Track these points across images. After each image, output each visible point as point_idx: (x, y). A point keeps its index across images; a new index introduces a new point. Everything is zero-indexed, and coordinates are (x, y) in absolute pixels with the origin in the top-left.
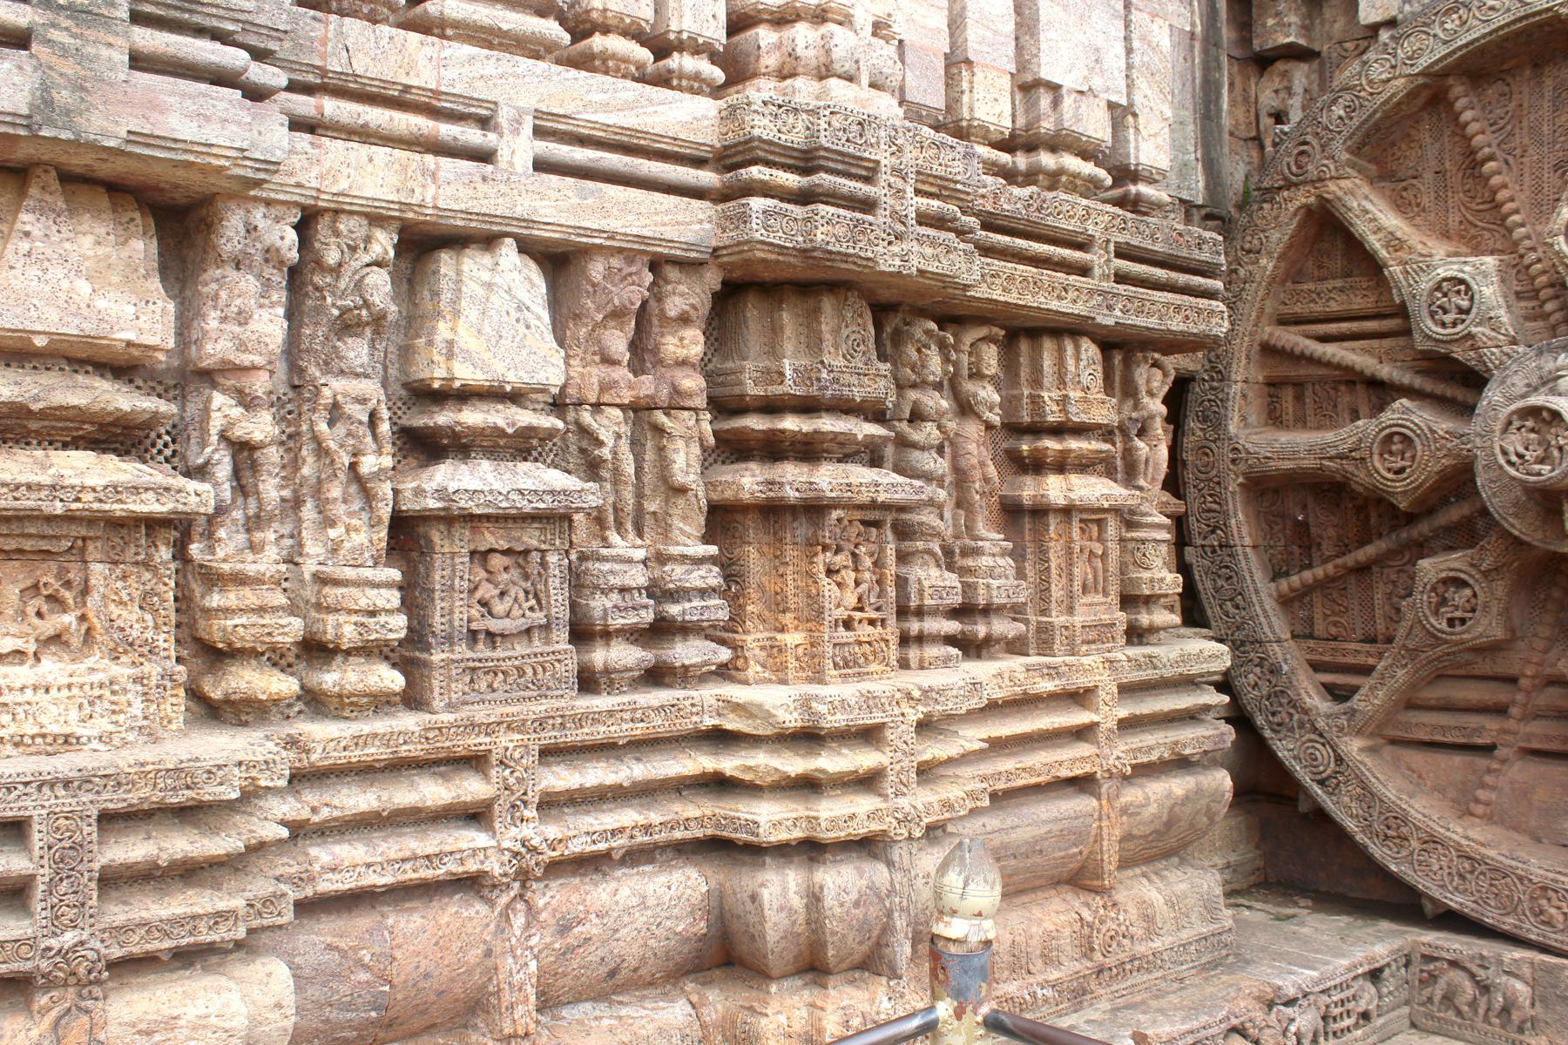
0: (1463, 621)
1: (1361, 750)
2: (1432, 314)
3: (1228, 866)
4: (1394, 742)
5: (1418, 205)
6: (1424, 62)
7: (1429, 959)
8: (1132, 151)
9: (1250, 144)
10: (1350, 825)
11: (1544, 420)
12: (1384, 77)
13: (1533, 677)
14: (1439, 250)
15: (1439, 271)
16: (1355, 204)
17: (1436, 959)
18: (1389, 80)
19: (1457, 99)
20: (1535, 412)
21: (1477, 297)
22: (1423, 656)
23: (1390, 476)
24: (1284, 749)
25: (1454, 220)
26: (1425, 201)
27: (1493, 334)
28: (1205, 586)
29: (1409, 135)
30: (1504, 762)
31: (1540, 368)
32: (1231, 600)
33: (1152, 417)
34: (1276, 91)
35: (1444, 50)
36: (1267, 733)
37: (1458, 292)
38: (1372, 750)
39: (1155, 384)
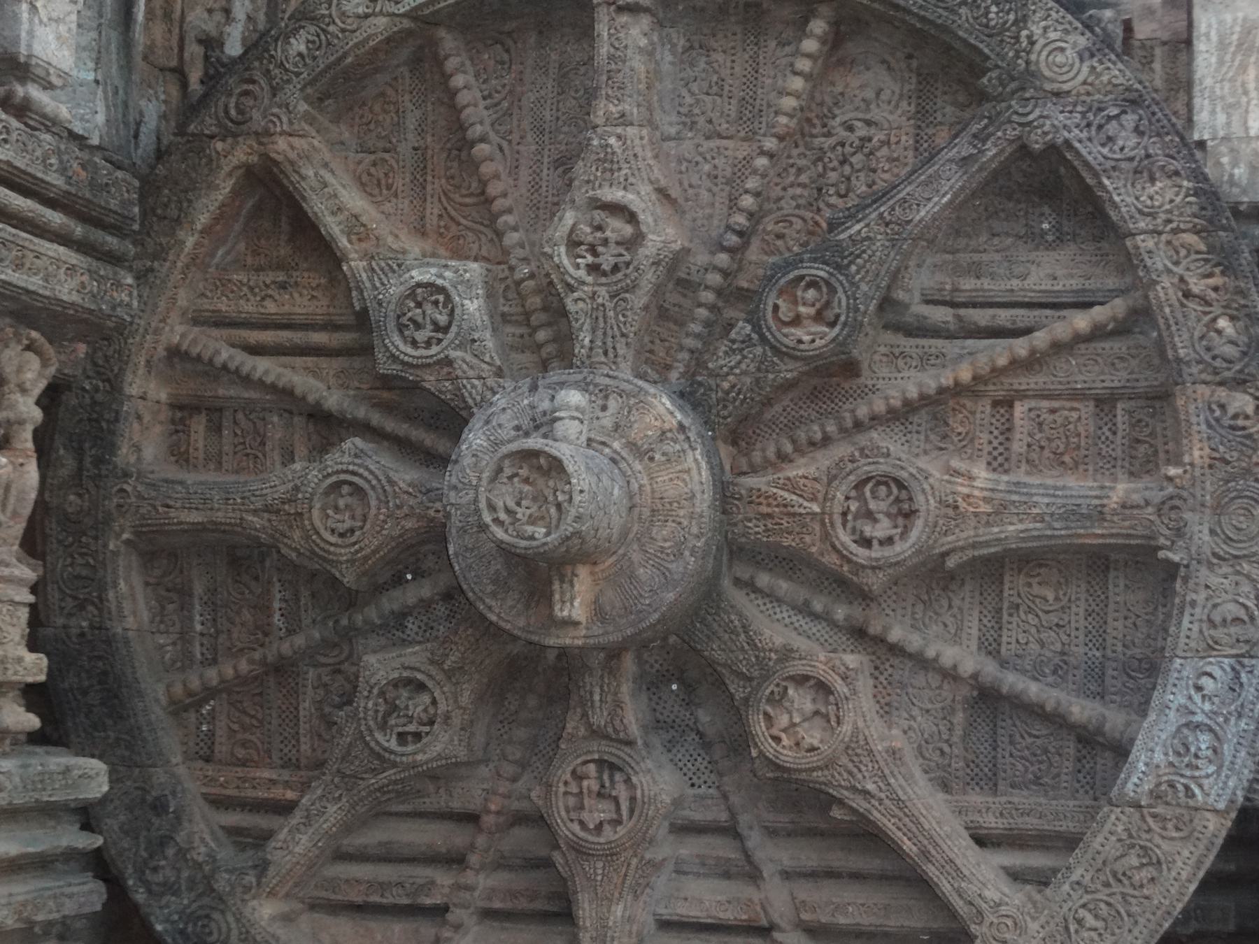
0: (417, 736)
1: (273, 918)
2: (401, 328)
4: (313, 907)
5: (389, 187)
8: (23, 34)
9: (169, 75)
11: (540, 468)
12: (360, 10)
13: (498, 813)
14: (415, 247)
15: (414, 273)
16: (311, 173)
18: (367, 16)
20: (529, 455)
21: (458, 311)
23: (333, 539)
25: (433, 210)
26: (398, 183)
27: (475, 361)
29: (383, 94)
30: (457, 927)
31: (533, 407)
33: (21, 422)
34: (210, 11)
37: (436, 303)
38: (287, 918)
39: (29, 375)
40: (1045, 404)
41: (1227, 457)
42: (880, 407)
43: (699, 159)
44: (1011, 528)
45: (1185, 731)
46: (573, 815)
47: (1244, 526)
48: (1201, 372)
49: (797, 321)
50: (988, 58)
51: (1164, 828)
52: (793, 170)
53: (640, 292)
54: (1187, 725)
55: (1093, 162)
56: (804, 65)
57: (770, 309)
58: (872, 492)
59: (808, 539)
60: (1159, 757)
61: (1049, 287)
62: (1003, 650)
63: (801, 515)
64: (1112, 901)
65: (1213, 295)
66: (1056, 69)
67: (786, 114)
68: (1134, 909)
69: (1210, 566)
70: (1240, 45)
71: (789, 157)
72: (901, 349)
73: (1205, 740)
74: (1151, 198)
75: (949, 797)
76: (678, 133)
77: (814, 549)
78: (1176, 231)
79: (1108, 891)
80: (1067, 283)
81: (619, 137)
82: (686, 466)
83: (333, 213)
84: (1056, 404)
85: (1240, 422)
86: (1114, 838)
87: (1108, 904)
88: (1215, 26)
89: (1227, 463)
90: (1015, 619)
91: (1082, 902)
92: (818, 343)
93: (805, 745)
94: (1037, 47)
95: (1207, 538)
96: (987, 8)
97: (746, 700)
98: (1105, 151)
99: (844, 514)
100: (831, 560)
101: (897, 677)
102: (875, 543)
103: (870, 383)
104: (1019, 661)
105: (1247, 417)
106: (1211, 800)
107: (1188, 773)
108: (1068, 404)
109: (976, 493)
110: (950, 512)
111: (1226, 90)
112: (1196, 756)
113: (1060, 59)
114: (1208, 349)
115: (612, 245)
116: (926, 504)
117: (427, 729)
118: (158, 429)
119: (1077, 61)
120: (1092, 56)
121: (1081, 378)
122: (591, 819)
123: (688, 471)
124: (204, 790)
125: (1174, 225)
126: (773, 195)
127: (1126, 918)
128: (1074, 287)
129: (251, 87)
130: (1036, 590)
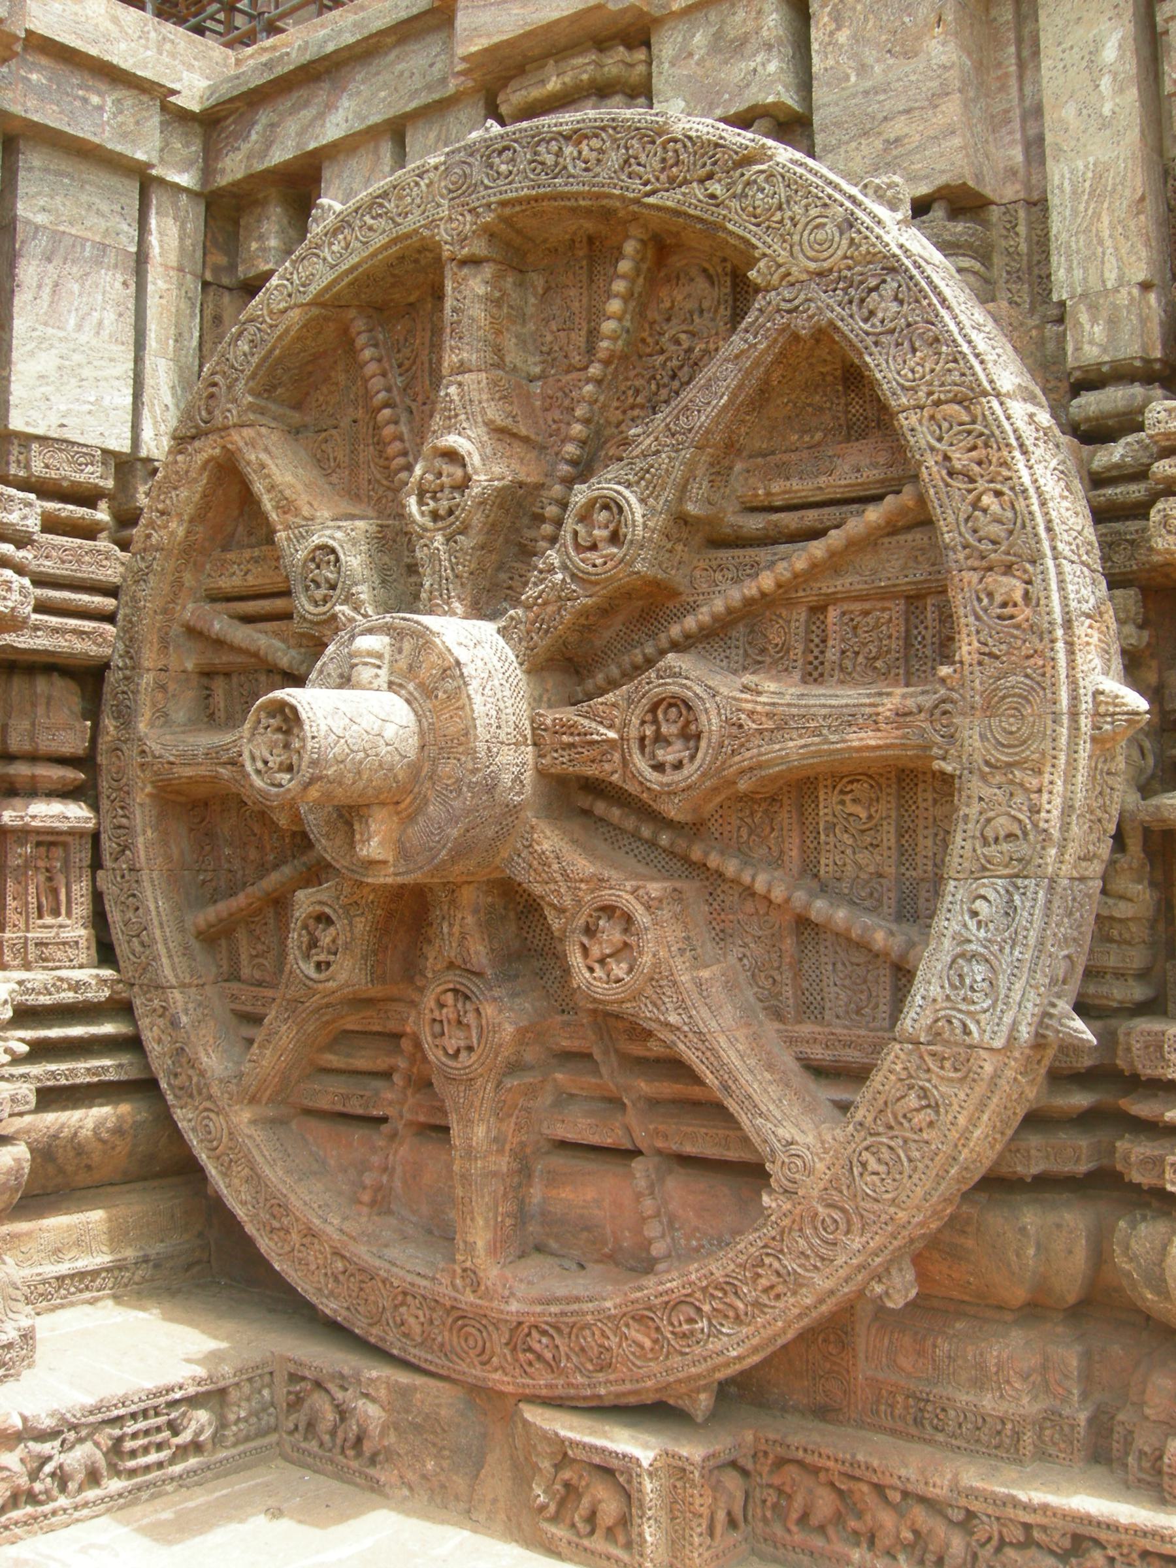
0: (328, 964)
1: (254, 1122)
2: (307, 588)
3: (146, 1260)
6: (314, 289)
7: (294, 1378)
10: (240, 1212)
12: (283, 305)
16: (253, 457)
17: (303, 1378)
18: (284, 312)
19: (359, 333)
22: (301, 1007)
24: (183, 1117)
28: (115, 916)
32: (138, 936)
35: (331, 276)
36: (170, 1098)
40: (857, 607)
41: (995, 650)
42: (690, 623)
43: (560, 394)
44: (791, 744)
45: (960, 961)
46: (437, 1041)
47: (1014, 729)
48: (967, 558)
49: (594, 547)
50: (755, 247)
51: (942, 1068)
52: (630, 392)
53: (473, 532)
54: (962, 955)
55: (855, 340)
56: (619, 286)
57: (569, 537)
58: (665, 713)
59: (607, 767)
60: (935, 990)
61: (853, 481)
62: (822, 872)
63: (597, 742)
64: (892, 1143)
65: (976, 468)
66: (817, 247)
67: (609, 338)
68: (916, 1154)
69: (983, 777)
70: (1092, 193)
71: (627, 379)
72: (719, 562)
73: (979, 971)
74: (913, 371)
75: (782, 1027)
76: (543, 371)
77: (615, 778)
78: (938, 403)
79: (891, 1133)
80: (871, 474)
81: (460, 384)
82: (460, 703)
83: (269, 491)
84: (867, 606)
85: (1009, 610)
86: (893, 1077)
87: (890, 1148)
88: (1067, 176)
89: (997, 657)
90: (831, 839)
91: (866, 1143)
92: (610, 564)
93: (612, 977)
94: (800, 227)
95: (978, 744)
96: (753, 197)
97: (564, 931)
98: (866, 327)
99: (642, 739)
100: (632, 788)
101: (728, 903)
102: (668, 767)
103: (691, 599)
104: (837, 884)
105: (1015, 605)
106: (987, 1036)
107: (963, 1007)
108: (879, 605)
109: (759, 708)
110: (734, 730)
111: (1081, 243)
112: (972, 989)
113: (820, 235)
114: (975, 531)
115: (447, 491)
116: (711, 723)
117: (332, 958)
118: (190, 694)
119: (837, 234)
120: (851, 226)
121: (885, 574)
122: (452, 1044)
123: (462, 708)
124: (233, 1006)
125: (935, 397)
126: (614, 420)
127: (906, 1164)
128: (878, 477)
129: (214, 389)
130: (851, 808)
